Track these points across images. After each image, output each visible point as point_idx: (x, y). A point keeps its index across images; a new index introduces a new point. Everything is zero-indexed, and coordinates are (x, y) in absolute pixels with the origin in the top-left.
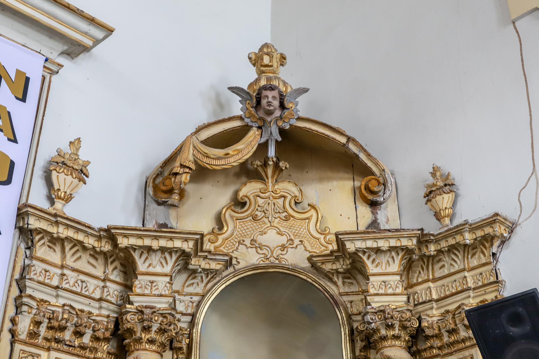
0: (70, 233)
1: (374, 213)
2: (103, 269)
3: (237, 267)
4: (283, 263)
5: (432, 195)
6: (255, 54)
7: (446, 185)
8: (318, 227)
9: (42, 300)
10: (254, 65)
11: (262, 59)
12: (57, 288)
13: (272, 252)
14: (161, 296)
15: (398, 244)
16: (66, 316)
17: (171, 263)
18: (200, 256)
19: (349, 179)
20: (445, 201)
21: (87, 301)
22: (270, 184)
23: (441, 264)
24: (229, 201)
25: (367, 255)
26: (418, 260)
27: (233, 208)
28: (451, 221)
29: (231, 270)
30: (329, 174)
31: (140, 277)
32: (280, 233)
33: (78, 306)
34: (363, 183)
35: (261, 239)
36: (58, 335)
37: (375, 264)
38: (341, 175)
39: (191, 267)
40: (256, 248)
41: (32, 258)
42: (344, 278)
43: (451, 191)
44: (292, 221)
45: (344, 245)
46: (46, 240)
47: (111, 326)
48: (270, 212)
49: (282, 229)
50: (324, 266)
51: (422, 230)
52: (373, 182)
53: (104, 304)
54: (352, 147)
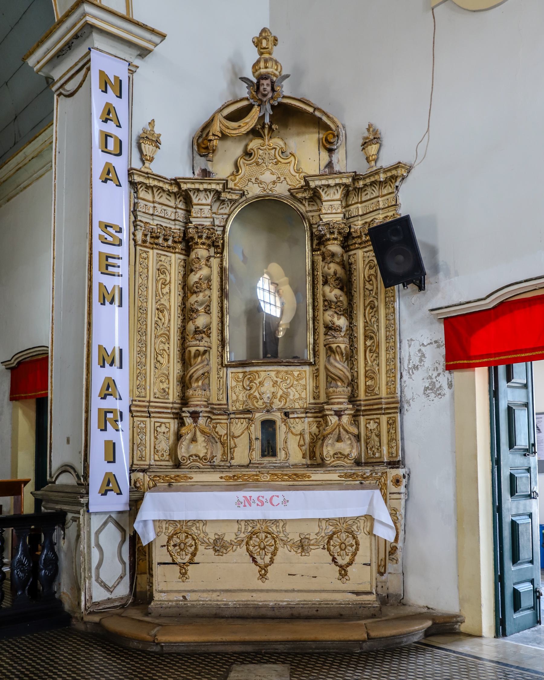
1: (330, 157)
2: (174, 202)
3: (248, 196)
4: (274, 193)
5: (366, 145)
6: (257, 38)
7: (375, 138)
8: (295, 168)
9: (146, 223)
10: (256, 47)
11: (261, 43)
12: (152, 215)
13: (268, 186)
14: (206, 218)
15: (341, 182)
16: (159, 231)
17: (211, 197)
18: (226, 192)
19: (316, 133)
20: (373, 150)
21: (168, 221)
22: (267, 140)
23: (366, 192)
24: (242, 153)
25: (322, 189)
26: (353, 190)
27: (244, 157)
28: (376, 162)
29: (244, 198)
30: (304, 129)
31: (194, 207)
32: (272, 174)
33: (164, 225)
34: (324, 137)
35: (262, 178)
36: (156, 241)
37: (326, 194)
38: (312, 130)
39: (221, 198)
40: (258, 183)
41: (138, 198)
42: (309, 202)
43: (377, 143)
44: (279, 165)
45: (309, 183)
47: (182, 235)
48: (267, 160)
49: (274, 171)
50: (297, 195)
51: (355, 172)
52: (331, 135)
53: (177, 222)
54: (317, 114)
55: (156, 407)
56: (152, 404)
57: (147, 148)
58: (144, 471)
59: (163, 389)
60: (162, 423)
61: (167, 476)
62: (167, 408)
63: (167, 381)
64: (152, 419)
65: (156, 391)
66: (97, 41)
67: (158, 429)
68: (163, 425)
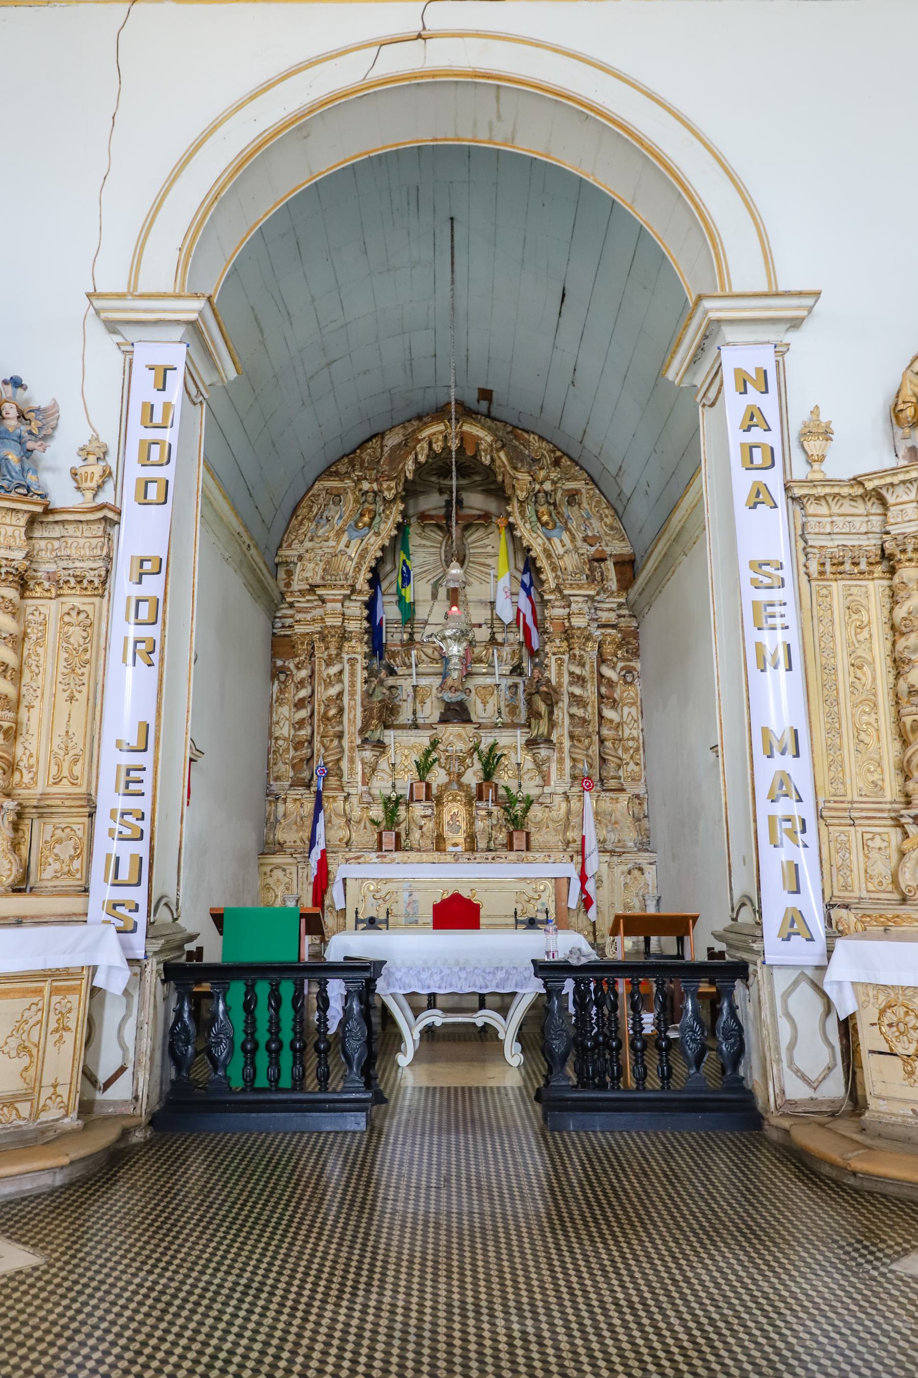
0: (828, 490)
36: (841, 568)
46: (812, 499)
47: (879, 552)
55: (862, 810)
56: (855, 805)
57: (814, 446)
58: (847, 907)
59: (873, 782)
60: (875, 834)
61: (881, 916)
62: (881, 810)
63: (879, 769)
64: (860, 829)
65: (861, 785)
66: (729, 334)
67: (870, 843)
68: (877, 837)
